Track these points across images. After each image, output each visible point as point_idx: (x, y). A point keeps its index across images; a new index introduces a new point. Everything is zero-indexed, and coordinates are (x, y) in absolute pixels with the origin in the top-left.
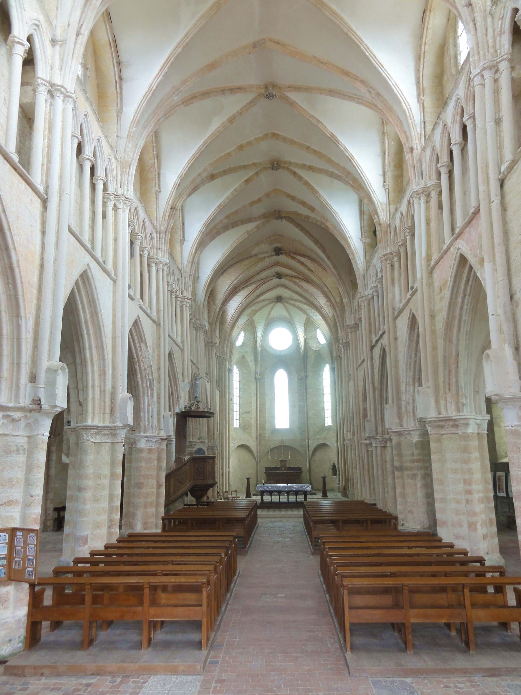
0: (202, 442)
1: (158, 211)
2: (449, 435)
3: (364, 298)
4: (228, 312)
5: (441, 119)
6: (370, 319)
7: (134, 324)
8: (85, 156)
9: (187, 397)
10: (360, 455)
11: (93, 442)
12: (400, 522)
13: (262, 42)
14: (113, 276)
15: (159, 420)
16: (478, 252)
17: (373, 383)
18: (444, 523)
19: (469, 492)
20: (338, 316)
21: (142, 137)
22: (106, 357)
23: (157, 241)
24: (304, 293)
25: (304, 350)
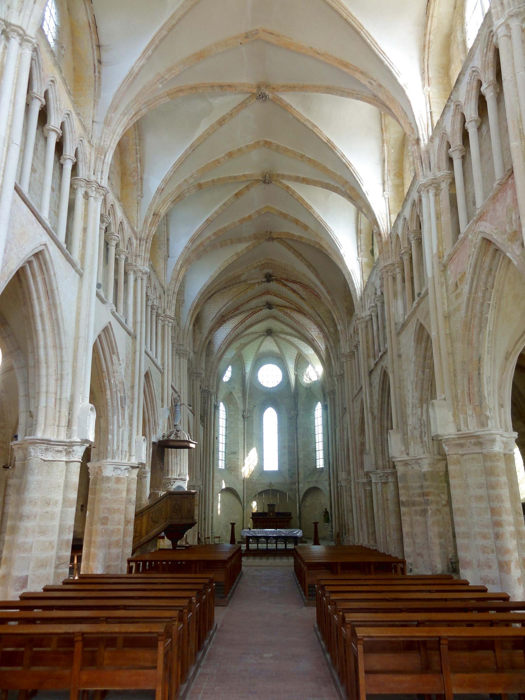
0: (181, 479)
1: (139, 217)
2: (471, 456)
3: (361, 320)
4: (215, 343)
5: (452, 101)
6: (367, 342)
7: (103, 330)
8: (50, 127)
9: (166, 425)
10: (357, 496)
11: (42, 459)
12: (408, 567)
13: (256, 32)
14: (79, 267)
15: (130, 445)
16: (507, 227)
17: (372, 414)
18: (468, 564)
19: (497, 524)
20: (331, 347)
21: (121, 124)
22: (65, 359)
23: (136, 247)
24: (295, 325)
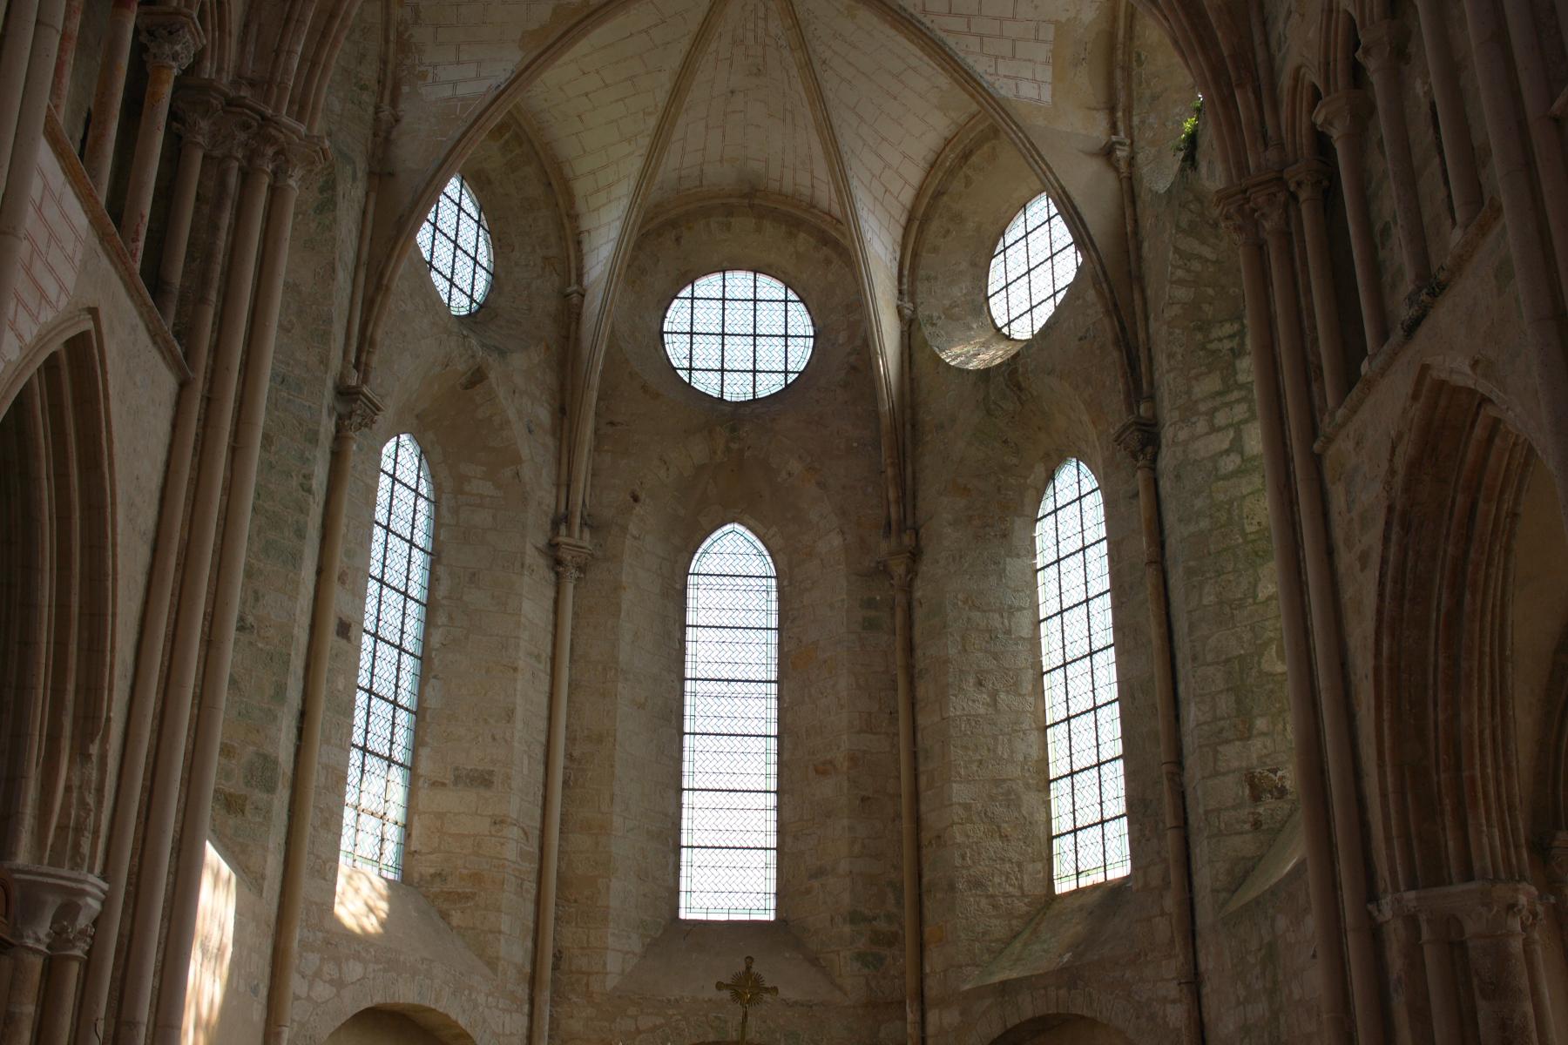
25: (901, 393)
